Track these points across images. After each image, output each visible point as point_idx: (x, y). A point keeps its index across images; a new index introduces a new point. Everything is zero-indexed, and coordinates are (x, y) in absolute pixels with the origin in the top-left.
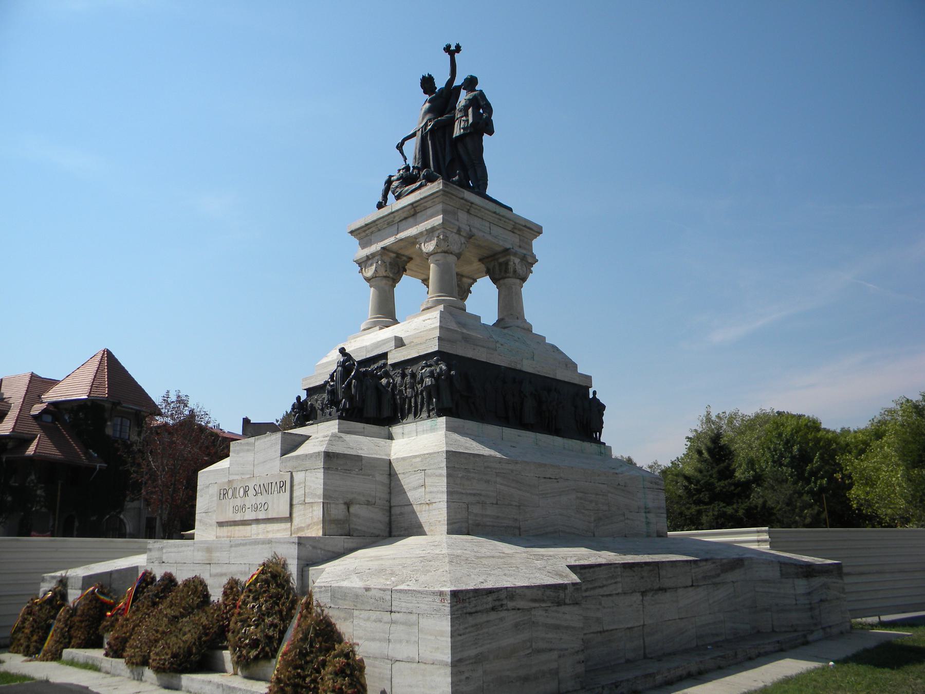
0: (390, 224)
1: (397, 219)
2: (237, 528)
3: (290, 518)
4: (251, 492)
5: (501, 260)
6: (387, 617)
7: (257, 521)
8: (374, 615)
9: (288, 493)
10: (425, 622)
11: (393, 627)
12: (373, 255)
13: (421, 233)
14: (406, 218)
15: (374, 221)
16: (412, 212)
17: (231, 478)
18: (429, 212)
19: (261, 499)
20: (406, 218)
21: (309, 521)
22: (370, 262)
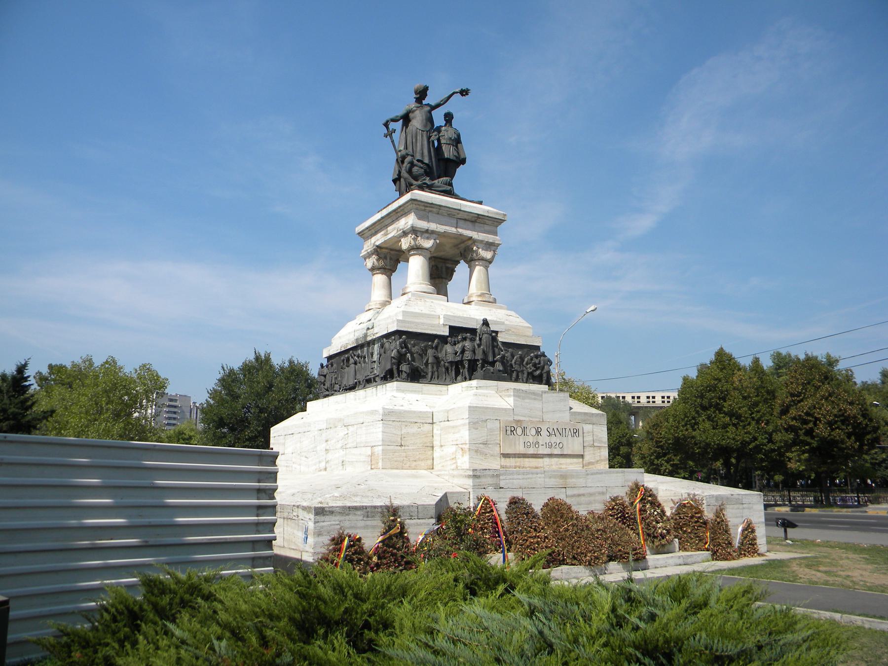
0: (450, 215)
1: (459, 216)
2: (527, 460)
3: (582, 456)
4: (544, 433)
5: (449, 265)
6: (741, 506)
7: (550, 456)
8: (736, 506)
9: (581, 438)
10: (755, 507)
11: (746, 510)
12: (433, 232)
13: (482, 241)
14: (465, 220)
15: (440, 206)
16: (473, 219)
17: (517, 418)
18: (487, 228)
19: (554, 439)
20: (465, 220)
21: (598, 458)
22: (427, 235)
